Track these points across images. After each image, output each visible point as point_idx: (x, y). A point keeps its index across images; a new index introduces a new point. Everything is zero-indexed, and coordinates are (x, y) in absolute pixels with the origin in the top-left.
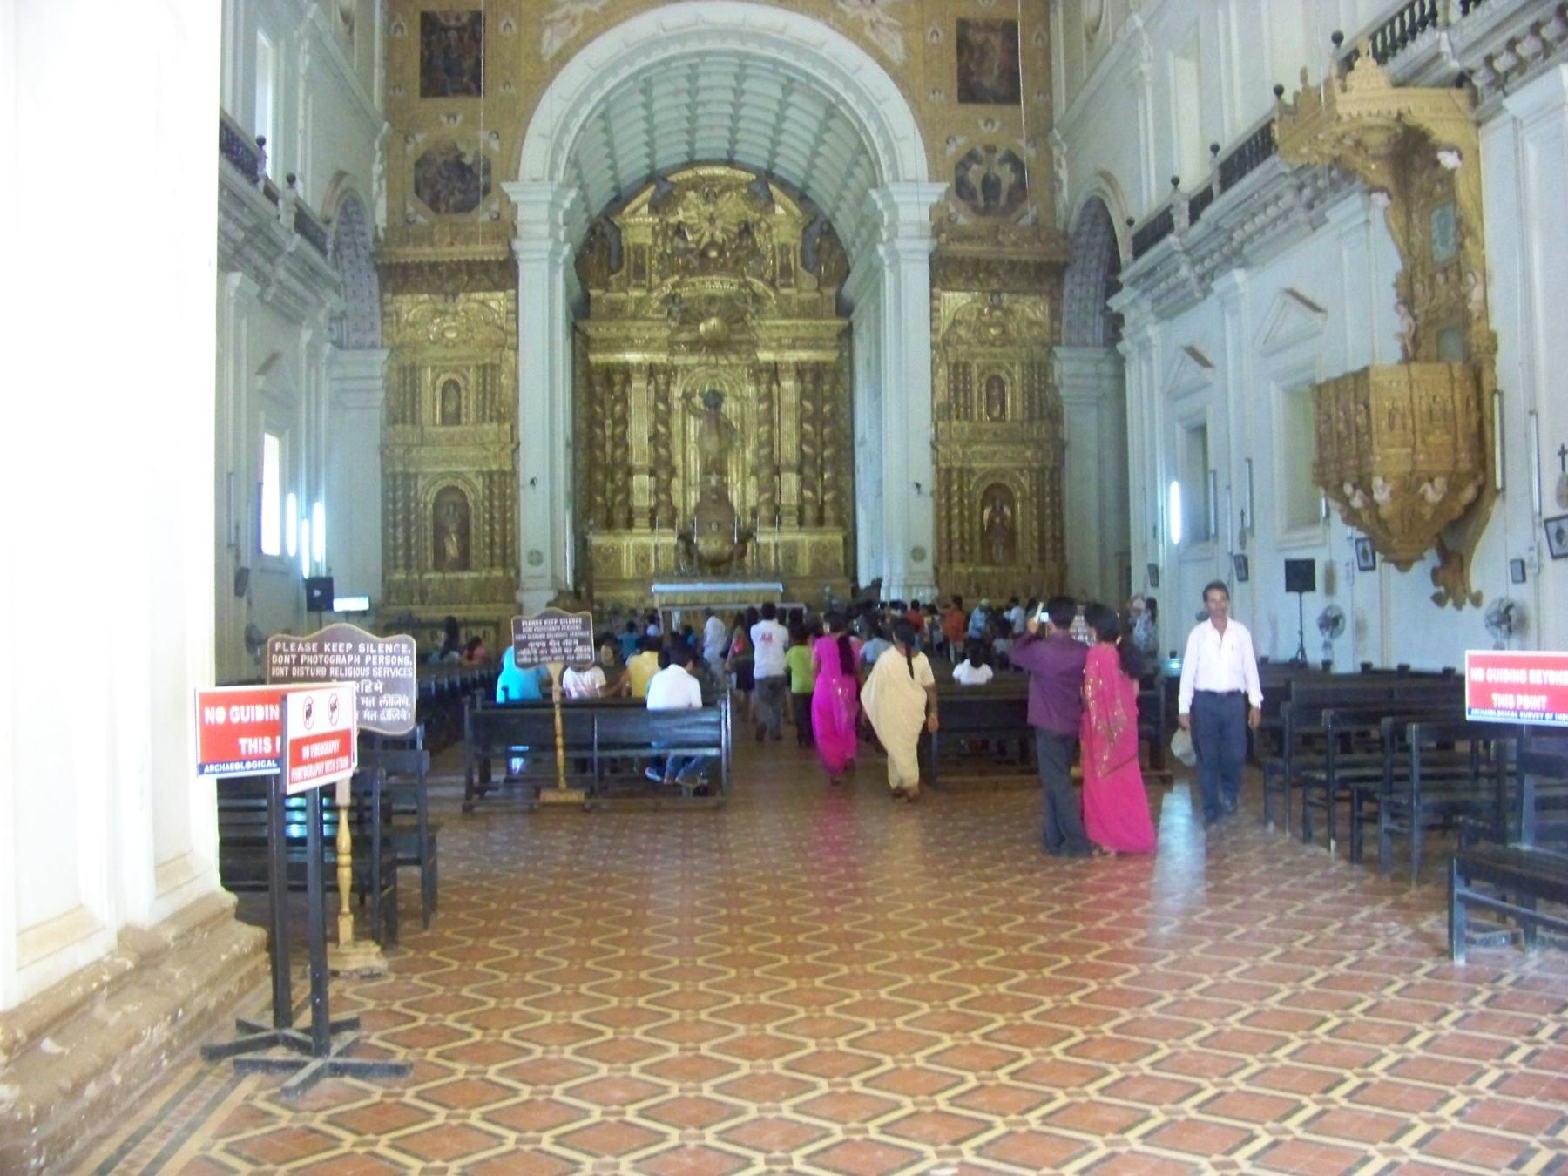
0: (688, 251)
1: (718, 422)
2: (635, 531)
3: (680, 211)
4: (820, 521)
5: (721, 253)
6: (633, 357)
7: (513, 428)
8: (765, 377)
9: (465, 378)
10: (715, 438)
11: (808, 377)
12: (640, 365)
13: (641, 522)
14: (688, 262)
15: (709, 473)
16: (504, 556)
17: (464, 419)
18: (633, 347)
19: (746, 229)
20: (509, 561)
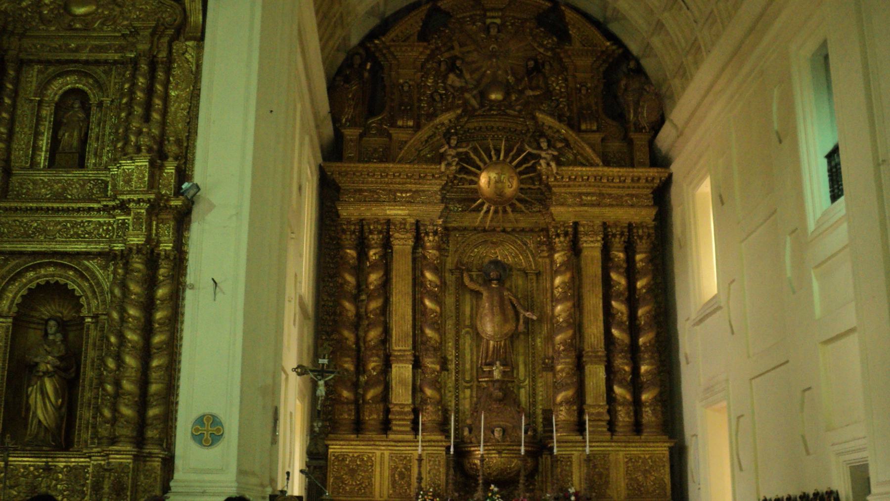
0: (463, 90)
1: (502, 299)
2: (392, 436)
3: (456, 44)
4: (637, 428)
5: (507, 94)
6: (396, 212)
7: (183, 175)
8: (560, 242)
9: (101, 86)
10: (497, 319)
11: (617, 243)
12: (403, 223)
13: (402, 424)
14: (466, 103)
15: (491, 364)
16: (142, 423)
17: (91, 161)
18: (395, 201)
19: (538, 68)
20: (151, 433)
